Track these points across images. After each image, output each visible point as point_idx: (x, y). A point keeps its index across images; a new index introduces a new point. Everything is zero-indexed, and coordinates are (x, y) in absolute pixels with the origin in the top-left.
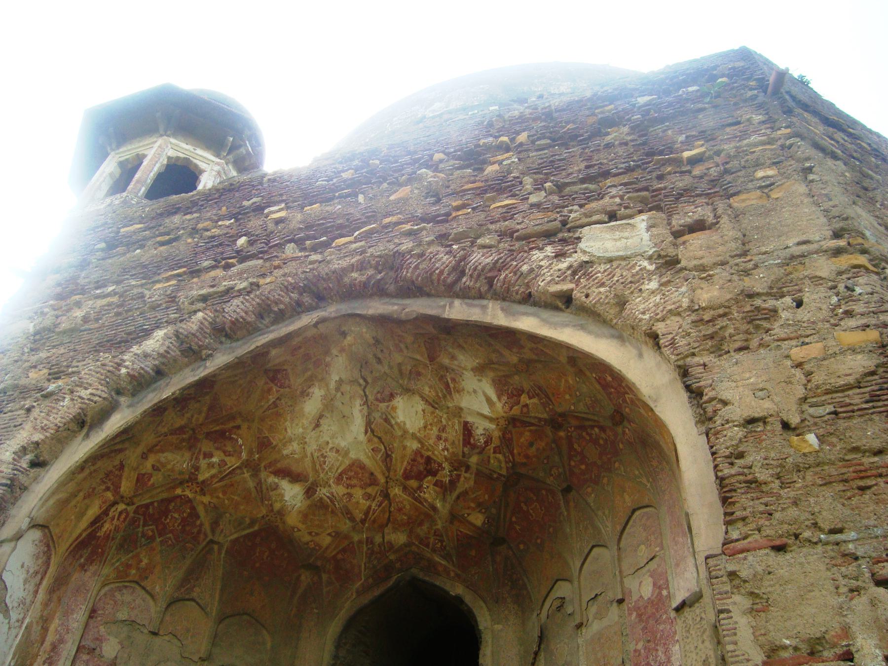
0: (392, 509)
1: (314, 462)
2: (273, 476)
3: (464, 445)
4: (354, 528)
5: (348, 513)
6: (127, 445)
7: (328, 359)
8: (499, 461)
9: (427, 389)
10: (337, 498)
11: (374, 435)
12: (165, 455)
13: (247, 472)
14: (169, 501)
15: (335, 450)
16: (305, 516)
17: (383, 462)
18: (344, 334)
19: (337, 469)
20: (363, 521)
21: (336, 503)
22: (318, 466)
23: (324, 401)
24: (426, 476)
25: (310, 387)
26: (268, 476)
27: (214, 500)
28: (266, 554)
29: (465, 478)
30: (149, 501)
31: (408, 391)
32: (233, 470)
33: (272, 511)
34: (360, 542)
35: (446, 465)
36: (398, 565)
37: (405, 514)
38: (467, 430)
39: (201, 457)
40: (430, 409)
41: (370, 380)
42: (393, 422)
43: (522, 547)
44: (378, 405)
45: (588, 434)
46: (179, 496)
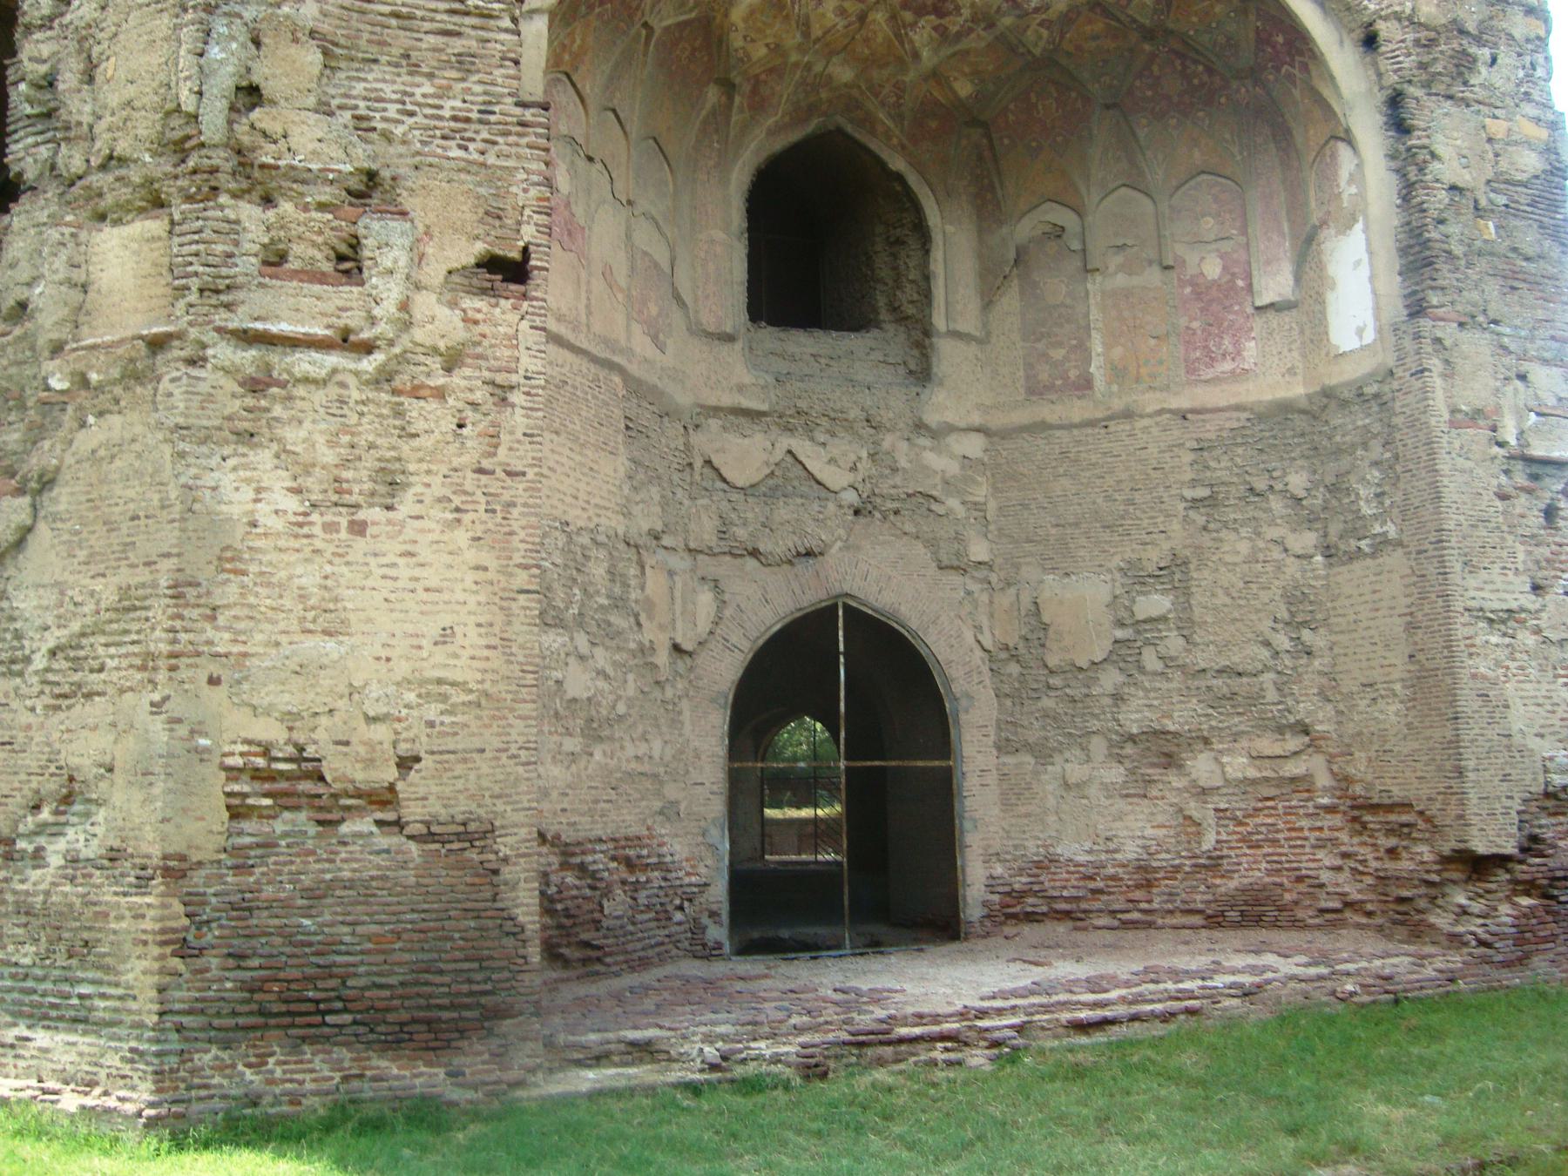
5: (805, 25)
8: (1040, 37)
20: (818, 40)
24: (928, 13)
34: (796, 65)
35: (966, 12)
36: (824, 107)
43: (1006, 141)
45: (1183, 64)
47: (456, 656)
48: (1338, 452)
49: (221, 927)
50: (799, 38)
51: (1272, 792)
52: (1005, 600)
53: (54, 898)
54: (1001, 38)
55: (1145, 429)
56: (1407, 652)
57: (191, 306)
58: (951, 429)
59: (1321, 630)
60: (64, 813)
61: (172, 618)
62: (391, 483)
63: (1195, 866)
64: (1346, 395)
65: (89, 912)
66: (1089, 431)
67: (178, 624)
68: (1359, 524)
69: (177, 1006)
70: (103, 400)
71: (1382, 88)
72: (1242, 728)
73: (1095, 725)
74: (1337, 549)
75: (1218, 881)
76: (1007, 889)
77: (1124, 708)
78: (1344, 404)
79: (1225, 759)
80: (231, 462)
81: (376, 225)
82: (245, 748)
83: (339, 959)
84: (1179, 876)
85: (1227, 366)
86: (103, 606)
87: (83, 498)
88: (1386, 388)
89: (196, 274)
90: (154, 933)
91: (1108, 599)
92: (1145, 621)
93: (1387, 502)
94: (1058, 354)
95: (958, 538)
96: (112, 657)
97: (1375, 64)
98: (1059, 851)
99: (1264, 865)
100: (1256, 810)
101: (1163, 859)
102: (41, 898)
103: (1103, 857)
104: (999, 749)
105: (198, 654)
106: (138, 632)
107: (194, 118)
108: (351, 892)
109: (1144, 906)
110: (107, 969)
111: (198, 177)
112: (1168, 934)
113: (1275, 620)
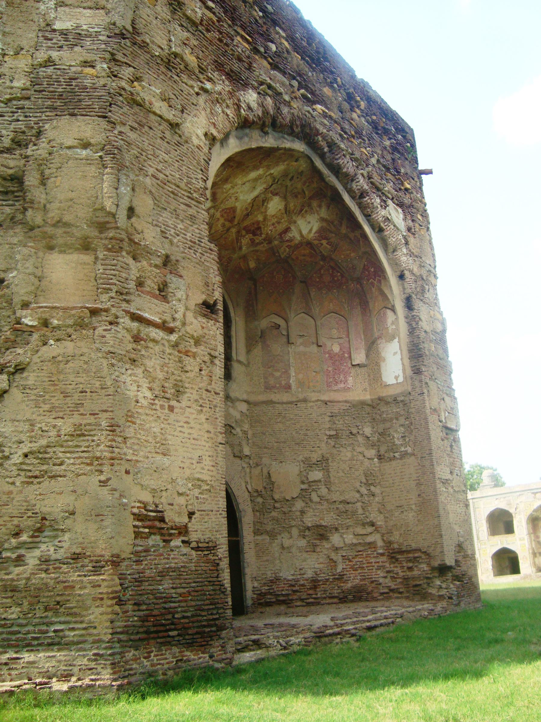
3: (279, 235)
8: (285, 251)
9: (292, 204)
18: (297, 161)
31: (285, 198)
35: (264, 236)
38: (287, 230)
40: (284, 211)
42: (265, 204)
43: (261, 288)
47: (203, 469)
48: (384, 421)
49: (132, 590)
51: (361, 548)
52: (256, 471)
53: (34, 581)
54: (272, 249)
55: (311, 407)
56: (417, 494)
57: (112, 298)
58: (238, 400)
59: (378, 487)
60: (37, 537)
61: (110, 441)
62: (179, 393)
63: (334, 579)
64: (389, 400)
65: (60, 587)
66: (290, 405)
67: (114, 444)
68: (394, 447)
69: (119, 630)
70: (58, 334)
71: (404, 293)
72: (350, 524)
73: (293, 523)
74: (384, 455)
75: (342, 585)
76: (259, 592)
77: (305, 516)
78: (387, 403)
79: (345, 536)
80: (129, 372)
81: (174, 279)
82: (139, 505)
83: (172, 605)
84: (328, 583)
85: (342, 385)
86: (63, 433)
87: (47, 379)
88: (407, 399)
89: (115, 284)
90: (108, 593)
91: (297, 472)
92: (312, 482)
93: (407, 440)
94: (277, 374)
95: (240, 445)
96: (69, 458)
97: (403, 285)
98: (281, 575)
99: (359, 577)
100: (356, 556)
101: (322, 577)
102: (24, 581)
103: (299, 577)
104: (255, 533)
105: (122, 459)
106: (88, 447)
107: (114, 215)
108: (175, 574)
109: (314, 596)
110: (75, 614)
111: (114, 241)
112: (327, 607)
113: (361, 482)
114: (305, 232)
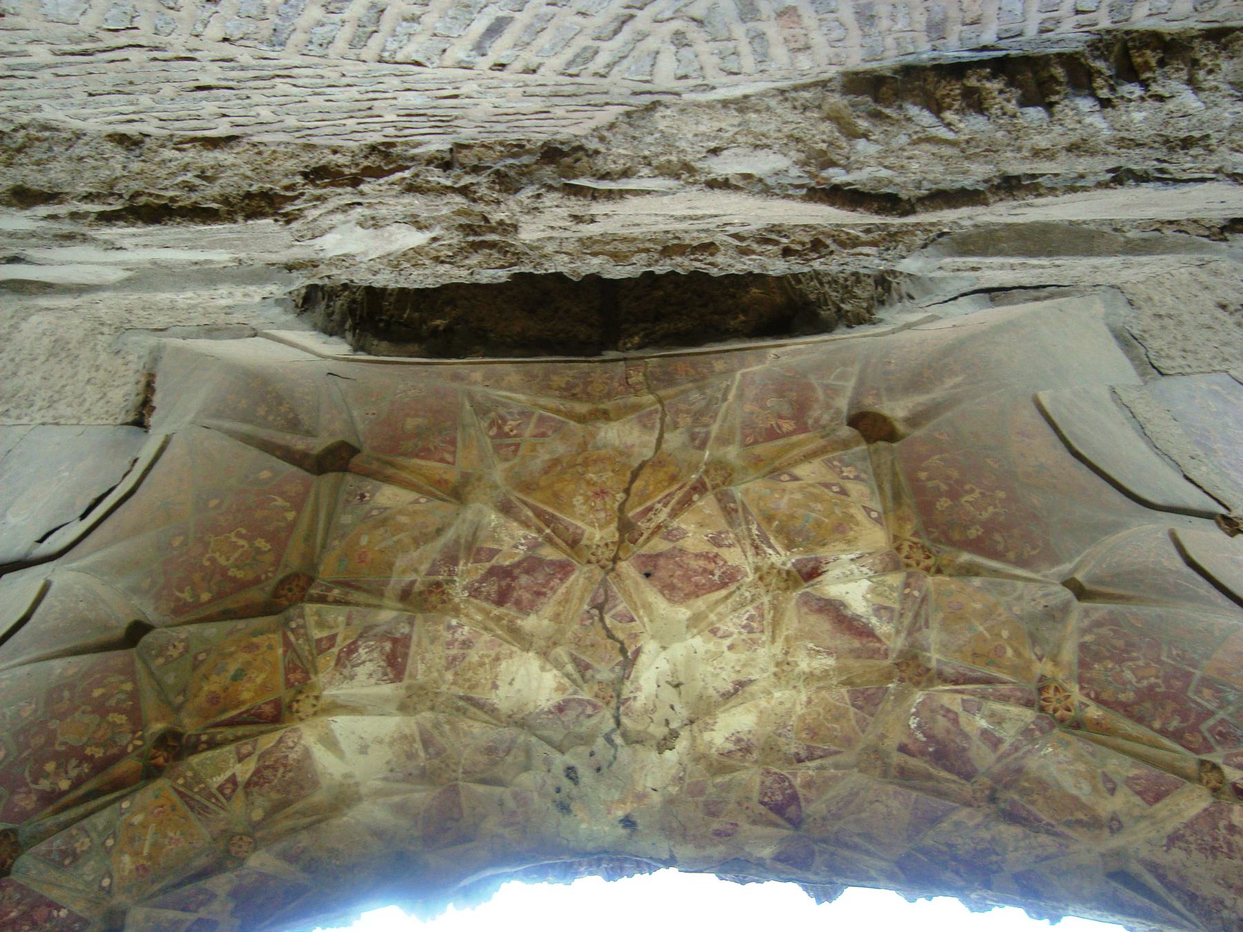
0: (620, 496)
1: (775, 624)
2: (878, 632)
3: (407, 639)
4: (728, 479)
5: (729, 510)
6: (1135, 868)
7: (674, 790)
8: (321, 624)
10: (748, 542)
11: (622, 643)
12: (1074, 792)
13: (929, 659)
14: (1126, 710)
15: (720, 633)
16: (841, 529)
17: (615, 598)
19: (727, 597)
20: (700, 488)
21: (755, 532)
22: (769, 617)
23: (711, 721)
25: (730, 752)
26: (888, 636)
27: (1028, 654)
28: (968, 498)
29: (416, 571)
30: (1166, 742)
32: (956, 682)
33: (910, 575)
34: (724, 441)
35: (458, 593)
37: (590, 483)
39: (1005, 747)
40: (475, 694)
41: (600, 741)
42: (570, 668)
44: (597, 696)
45: (90, 759)
46: (1099, 701)
50: (738, 491)
114: (341, 724)
